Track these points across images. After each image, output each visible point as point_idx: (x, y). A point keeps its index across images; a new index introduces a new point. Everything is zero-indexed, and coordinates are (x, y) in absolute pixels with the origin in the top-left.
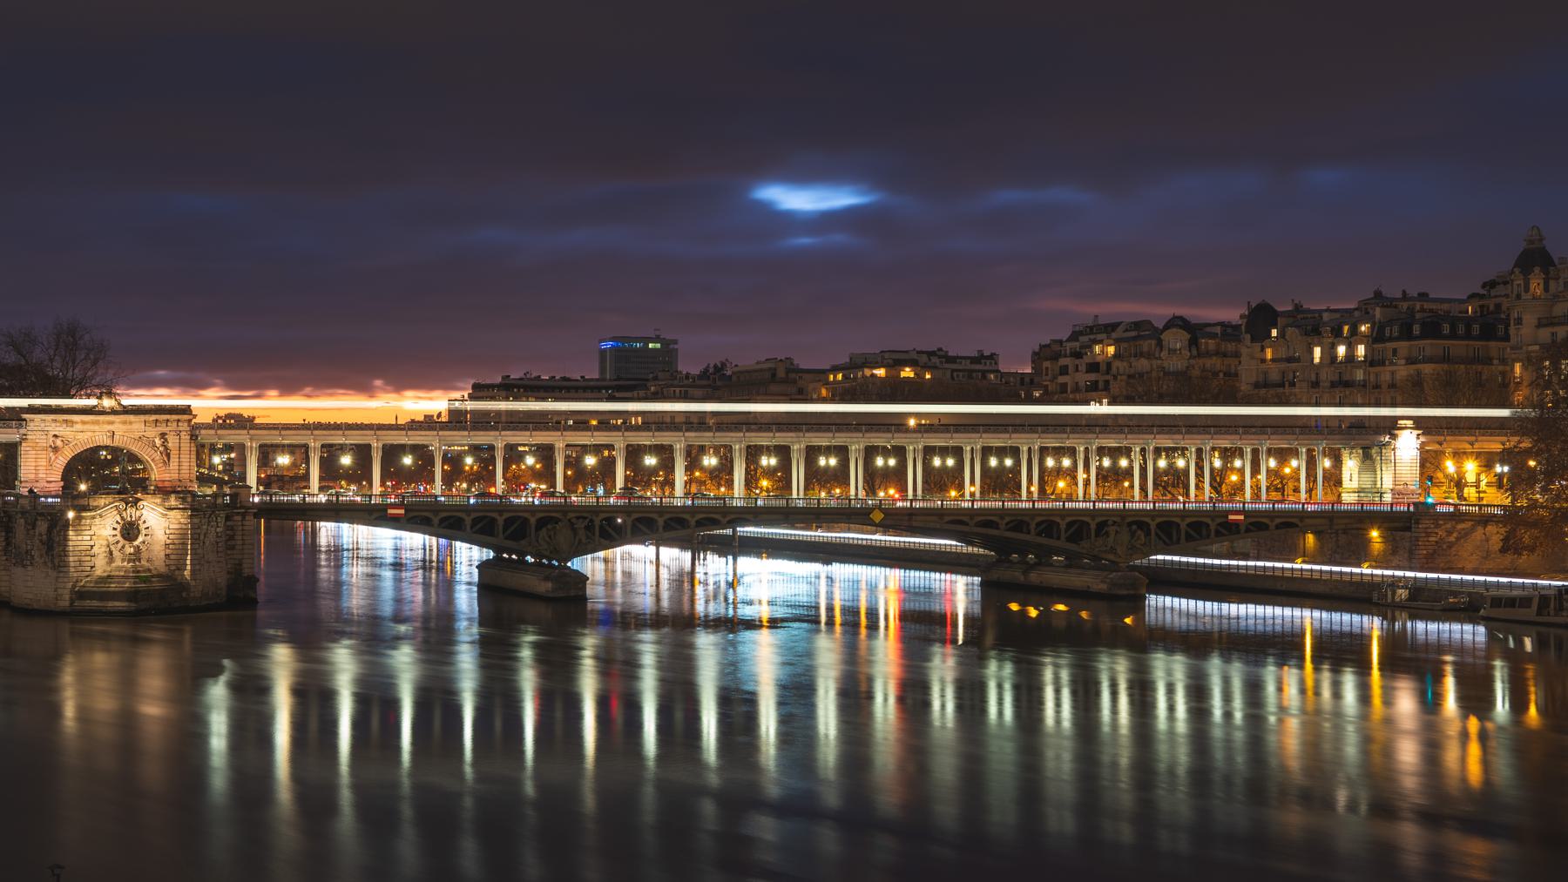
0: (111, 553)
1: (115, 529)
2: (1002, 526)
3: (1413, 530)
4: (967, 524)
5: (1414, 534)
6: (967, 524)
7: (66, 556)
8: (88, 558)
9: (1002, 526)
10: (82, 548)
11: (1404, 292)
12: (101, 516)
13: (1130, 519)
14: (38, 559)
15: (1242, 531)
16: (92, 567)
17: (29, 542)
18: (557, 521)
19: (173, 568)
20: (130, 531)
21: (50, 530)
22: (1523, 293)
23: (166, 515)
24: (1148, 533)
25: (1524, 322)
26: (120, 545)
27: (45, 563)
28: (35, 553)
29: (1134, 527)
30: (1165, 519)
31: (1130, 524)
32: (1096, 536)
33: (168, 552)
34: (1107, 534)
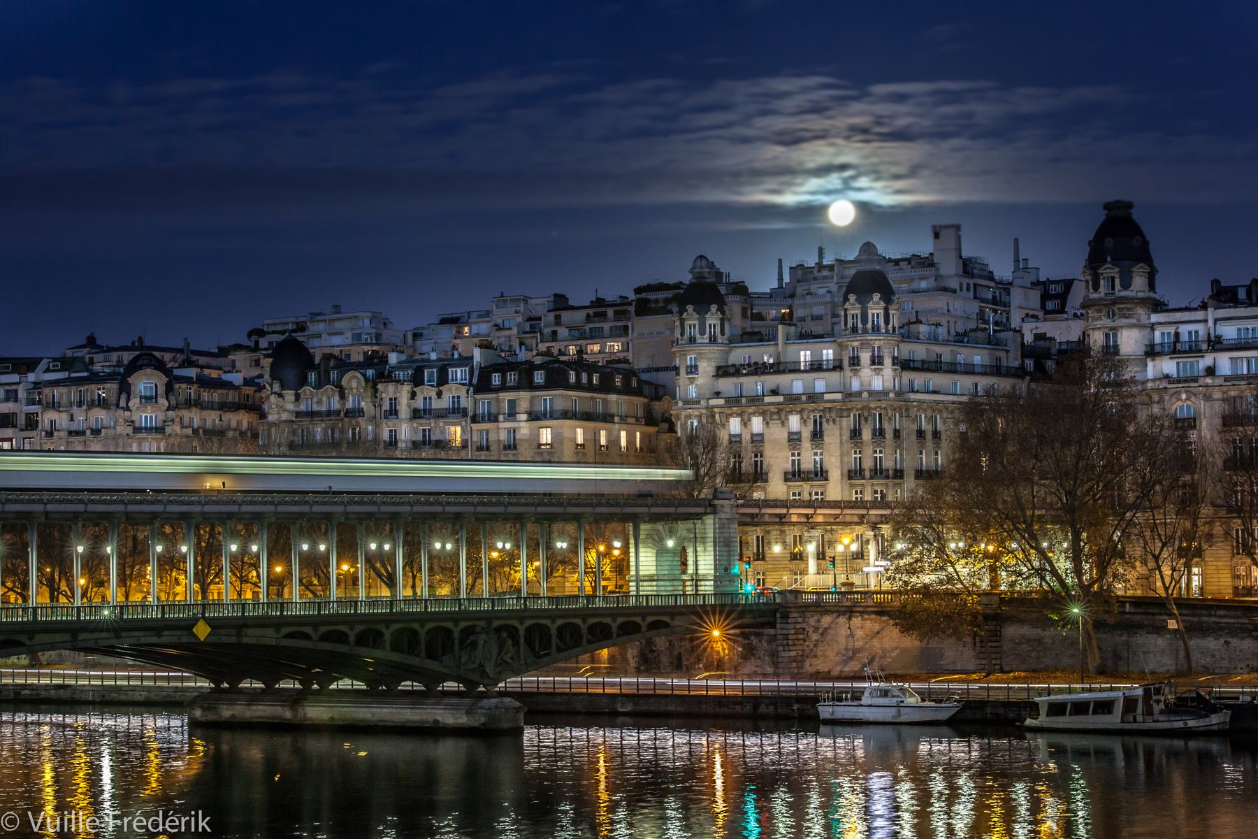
2: (352, 638)
3: (778, 626)
4: (307, 637)
5: (779, 632)
6: (307, 637)
9: (352, 638)
11: (140, 339)
13: (496, 624)
15: (615, 636)
22: (698, 336)
24: (516, 643)
25: (700, 369)
29: (505, 635)
30: (330, 628)
31: (498, 630)
32: (461, 648)
34: (474, 645)
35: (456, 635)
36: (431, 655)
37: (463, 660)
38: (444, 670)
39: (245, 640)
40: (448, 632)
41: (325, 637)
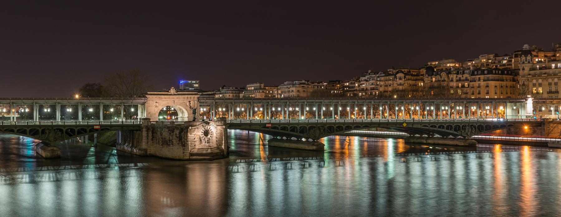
0: (201, 140)
1: (202, 132)
3: (542, 126)
4: (428, 126)
6: (428, 126)
7: (187, 141)
8: (194, 142)
9: (437, 127)
10: (192, 139)
12: (197, 128)
14: (175, 143)
16: (195, 145)
17: (170, 137)
18: (315, 127)
19: (218, 145)
20: (206, 133)
21: (180, 133)
23: (216, 127)
24: (475, 129)
26: (203, 138)
27: (178, 144)
28: (174, 141)
33: (217, 140)
34: (465, 129)
35: (461, 127)
36: (455, 130)
37: (463, 132)
38: (458, 134)
39: (414, 127)
40: (459, 126)
41: (432, 126)
